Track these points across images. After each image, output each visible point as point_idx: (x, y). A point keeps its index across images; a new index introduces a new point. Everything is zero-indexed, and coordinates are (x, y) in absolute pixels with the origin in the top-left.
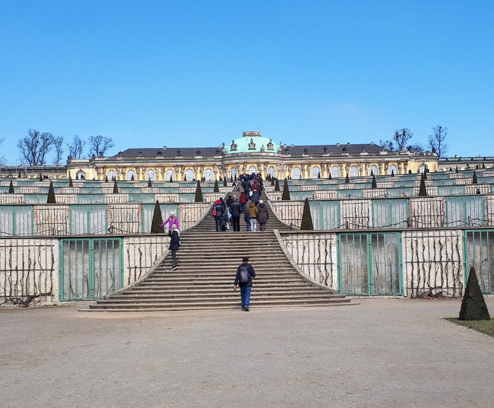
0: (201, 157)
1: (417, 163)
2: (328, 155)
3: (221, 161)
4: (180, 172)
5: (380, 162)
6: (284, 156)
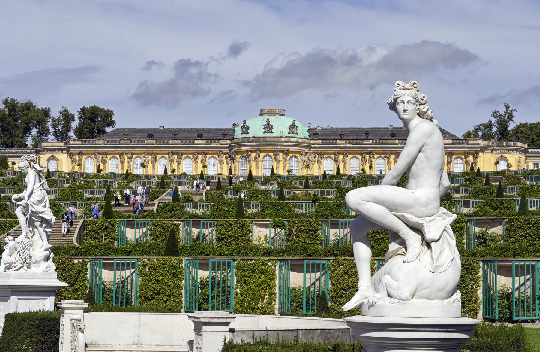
0: (203, 142)
1: (494, 155)
2: (371, 141)
3: (228, 147)
4: (175, 161)
6: (312, 142)
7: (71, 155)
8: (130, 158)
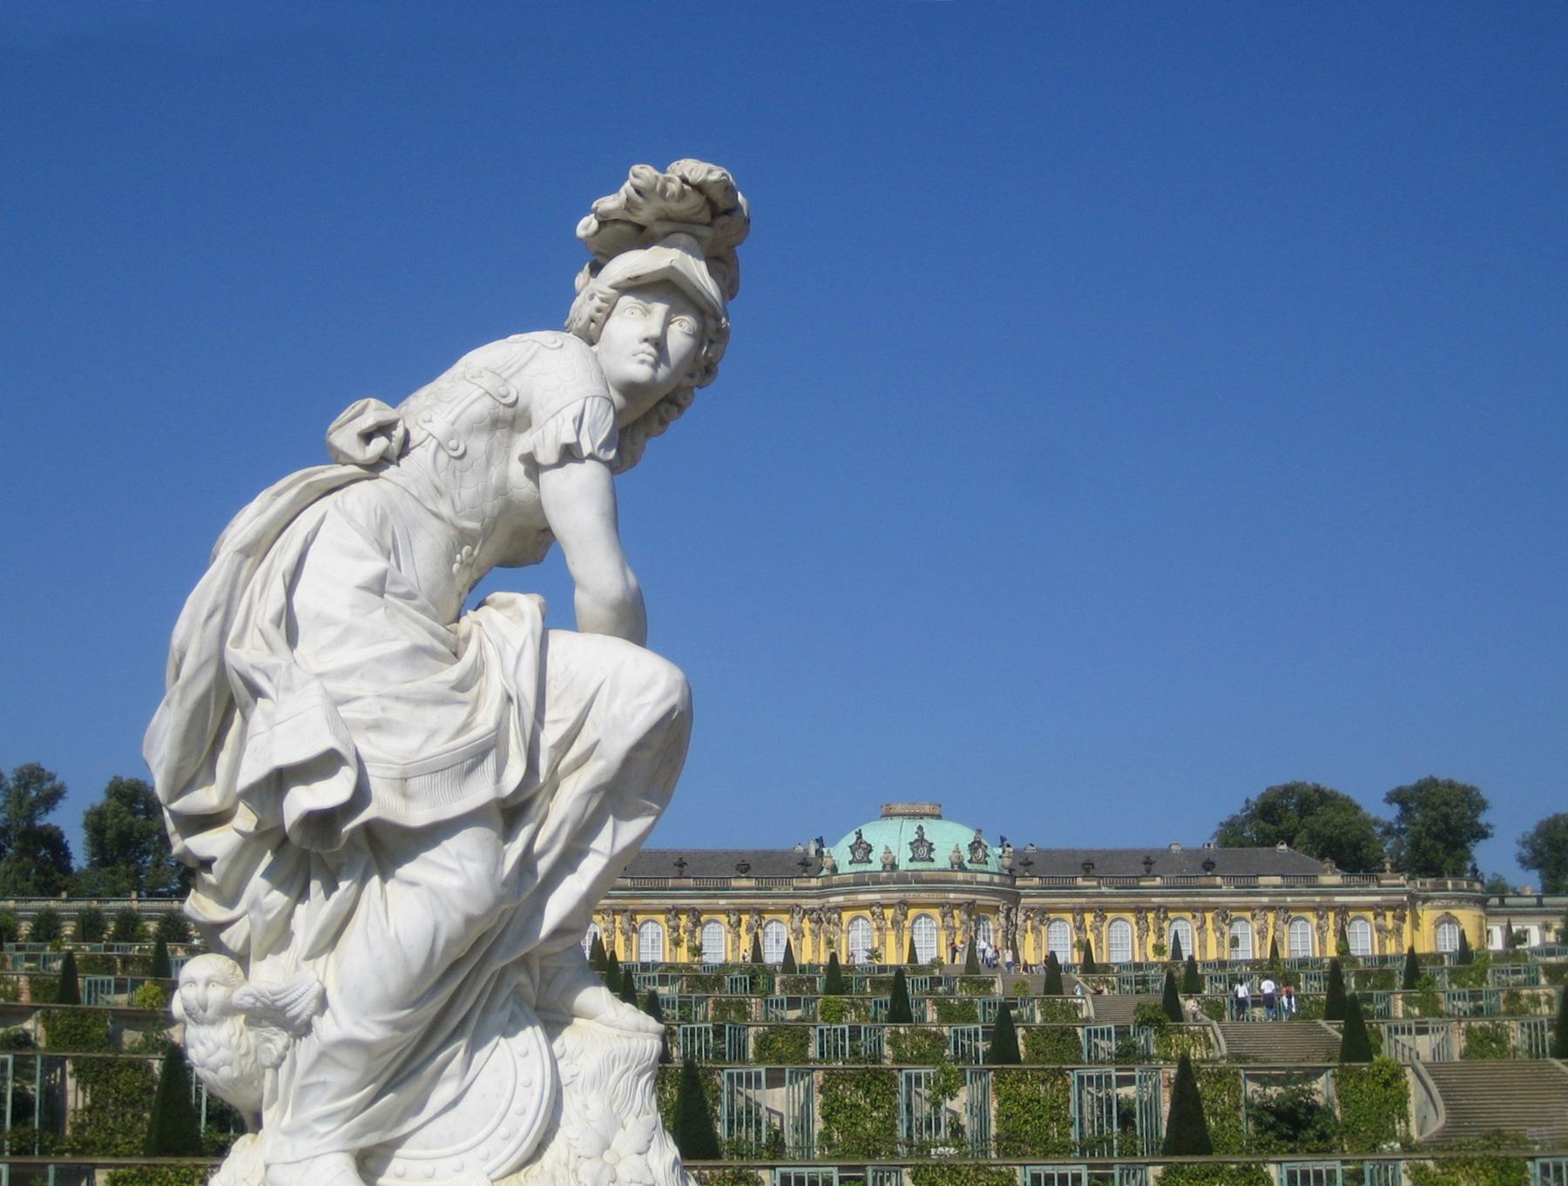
2: (1158, 881)
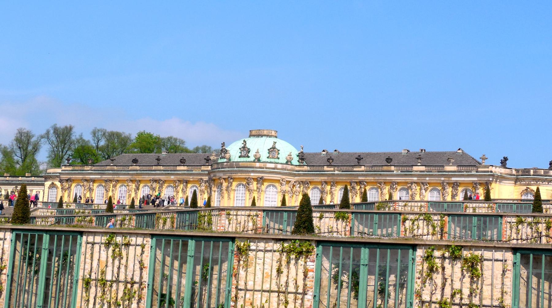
0: (185, 168)
1: (519, 187)
2: (363, 168)
5: (443, 183)
7: (61, 181)
8: (115, 186)
